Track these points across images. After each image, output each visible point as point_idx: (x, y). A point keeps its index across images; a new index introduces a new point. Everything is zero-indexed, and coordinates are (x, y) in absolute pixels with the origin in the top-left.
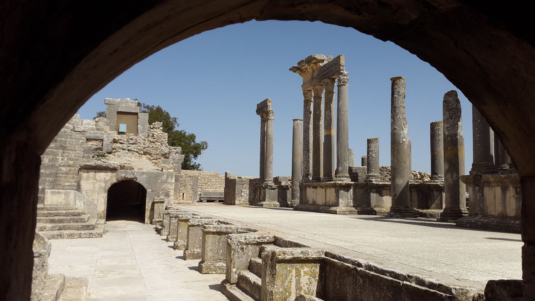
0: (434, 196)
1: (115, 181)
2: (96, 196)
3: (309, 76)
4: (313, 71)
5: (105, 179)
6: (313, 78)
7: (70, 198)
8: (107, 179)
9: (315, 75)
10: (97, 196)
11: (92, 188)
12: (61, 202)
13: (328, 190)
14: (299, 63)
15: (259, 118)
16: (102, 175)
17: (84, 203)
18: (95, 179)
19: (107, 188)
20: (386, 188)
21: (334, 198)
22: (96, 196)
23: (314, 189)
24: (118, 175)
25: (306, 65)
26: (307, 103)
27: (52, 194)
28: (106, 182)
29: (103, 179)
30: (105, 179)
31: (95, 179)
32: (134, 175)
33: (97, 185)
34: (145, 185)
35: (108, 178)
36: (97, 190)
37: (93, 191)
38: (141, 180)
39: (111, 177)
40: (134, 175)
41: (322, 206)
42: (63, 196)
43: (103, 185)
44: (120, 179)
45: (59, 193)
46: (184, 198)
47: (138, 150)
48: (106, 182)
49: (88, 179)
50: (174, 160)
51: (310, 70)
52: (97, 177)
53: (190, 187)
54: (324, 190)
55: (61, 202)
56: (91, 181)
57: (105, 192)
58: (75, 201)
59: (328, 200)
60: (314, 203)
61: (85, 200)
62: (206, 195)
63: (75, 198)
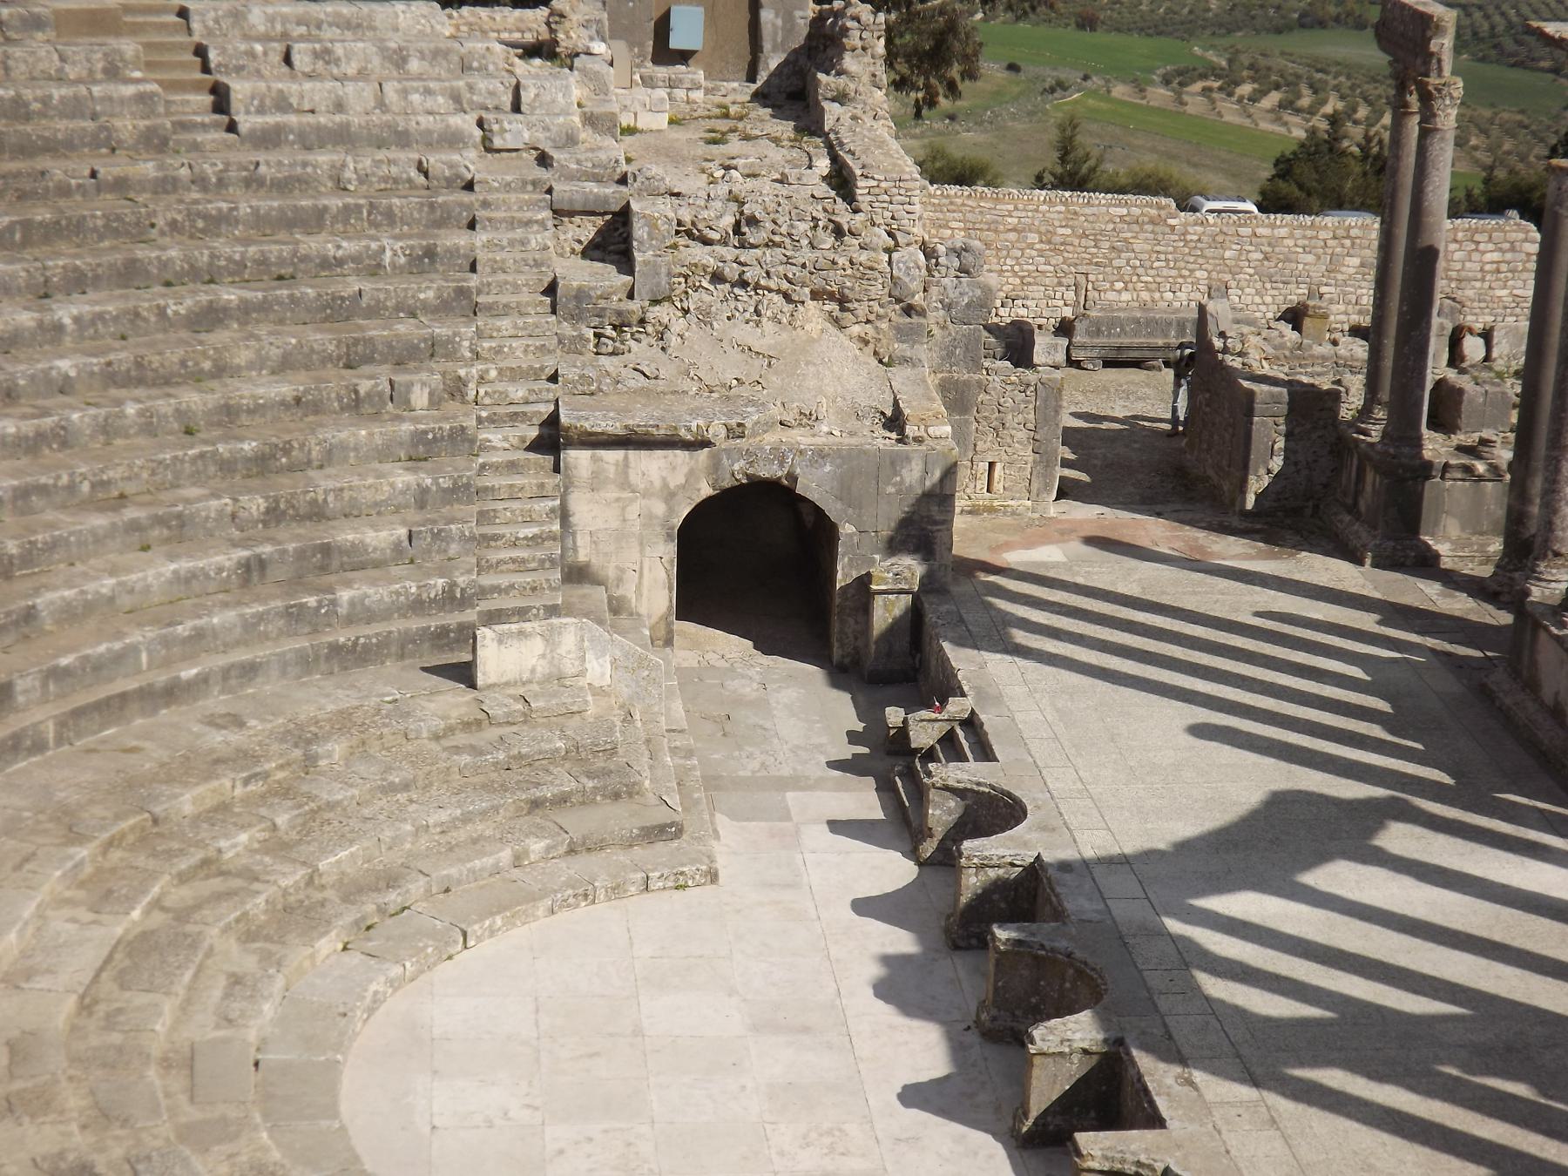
1: (706, 491)
2: (631, 556)
5: (665, 485)
7: (562, 650)
8: (674, 483)
10: (636, 556)
11: (615, 524)
12: (533, 671)
16: (651, 466)
17: (614, 662)
18: (625, 484)
19: (678, 521)
22: (631, 556)
24: (715, 466)
27: (500, 642)
28: (670, 496)
29: (658, 484)
30: (665, 485)
31: (625, 484)
32: (781, 465)
33: (633, 511)
34: (832, 509)
35: (677, 479)
36: (637, 529)
37: (620, 536)
38: (814, 486)
39: (691, 474)
40: (781, 465)
42: (538, 645)
43: (659, 508)
44: (727, 483)
45: (521, 633)
46: (998, 486)
47: (785, 285)
48: (670, 496)
49: (596, 482)
50: (948, 307)
52: (634, 478)
53: (1022, 435)
55: (533, 671)
56: (611, 493)
58: (583, 659)
61: (618, 654)
62: (1098, 332)
63: (581, 649)
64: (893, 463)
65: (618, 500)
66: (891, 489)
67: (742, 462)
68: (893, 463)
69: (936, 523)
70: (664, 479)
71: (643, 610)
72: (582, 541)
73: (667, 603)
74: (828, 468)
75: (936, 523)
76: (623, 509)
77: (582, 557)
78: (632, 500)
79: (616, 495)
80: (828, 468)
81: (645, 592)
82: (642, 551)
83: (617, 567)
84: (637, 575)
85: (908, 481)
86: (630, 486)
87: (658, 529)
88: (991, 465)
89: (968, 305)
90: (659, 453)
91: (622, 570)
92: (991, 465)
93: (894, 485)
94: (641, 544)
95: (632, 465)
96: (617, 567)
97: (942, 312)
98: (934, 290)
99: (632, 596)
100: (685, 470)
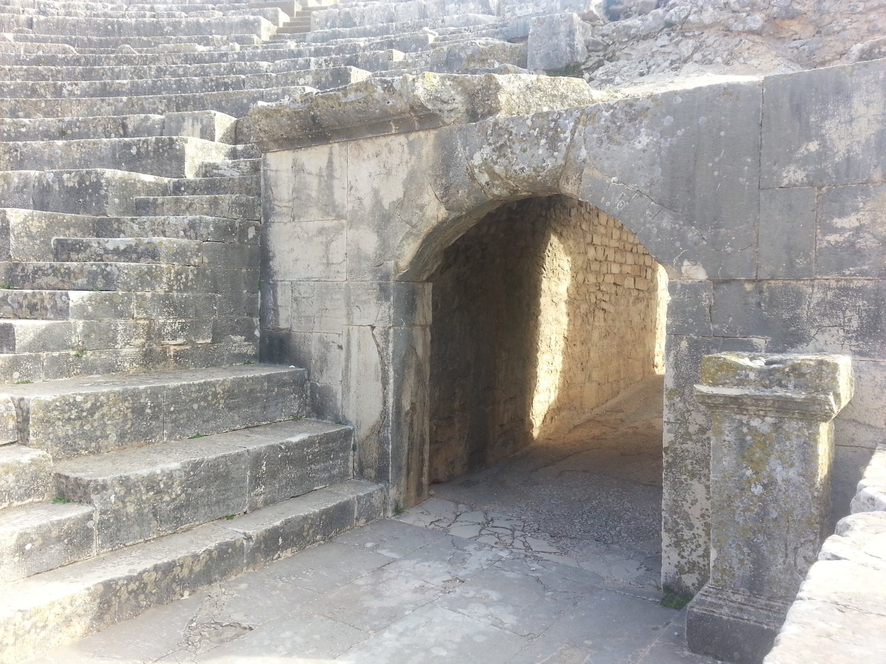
1: (434, 211)
5: (378, 203)
24: (446, 161)
28: (383, 220)
29: (368, 202)
30: (378, 203)
33: (339, 248)
43: (370, 242)
48: (383, 220)
52: (340, 195)
57: (383, 292)
64: (798, 110)
65: (321, 231)
66: (794, 175)
67: (487, 150)
70: (376, 192)
71: (351, 415)
72: (283, 297)
73: (379, 407)
74: (643, 140)
76: (327, 245)
77: (283, 325)
78: (338, 231)
79: (319, 224)
80: (643, 140)
81: (353, 383)
82: (349, 315)
83: (321, 340)
84: (343, 354)
85: (841, 147)
86: (335, 207)
87: (369, 277)
90: (369, 146)
91: (326, 345)
93: (805, 161)
94: (348, 305)
95: (337, 174)
96: (321, 340)
99: (338, 388)
100: (402, 174)
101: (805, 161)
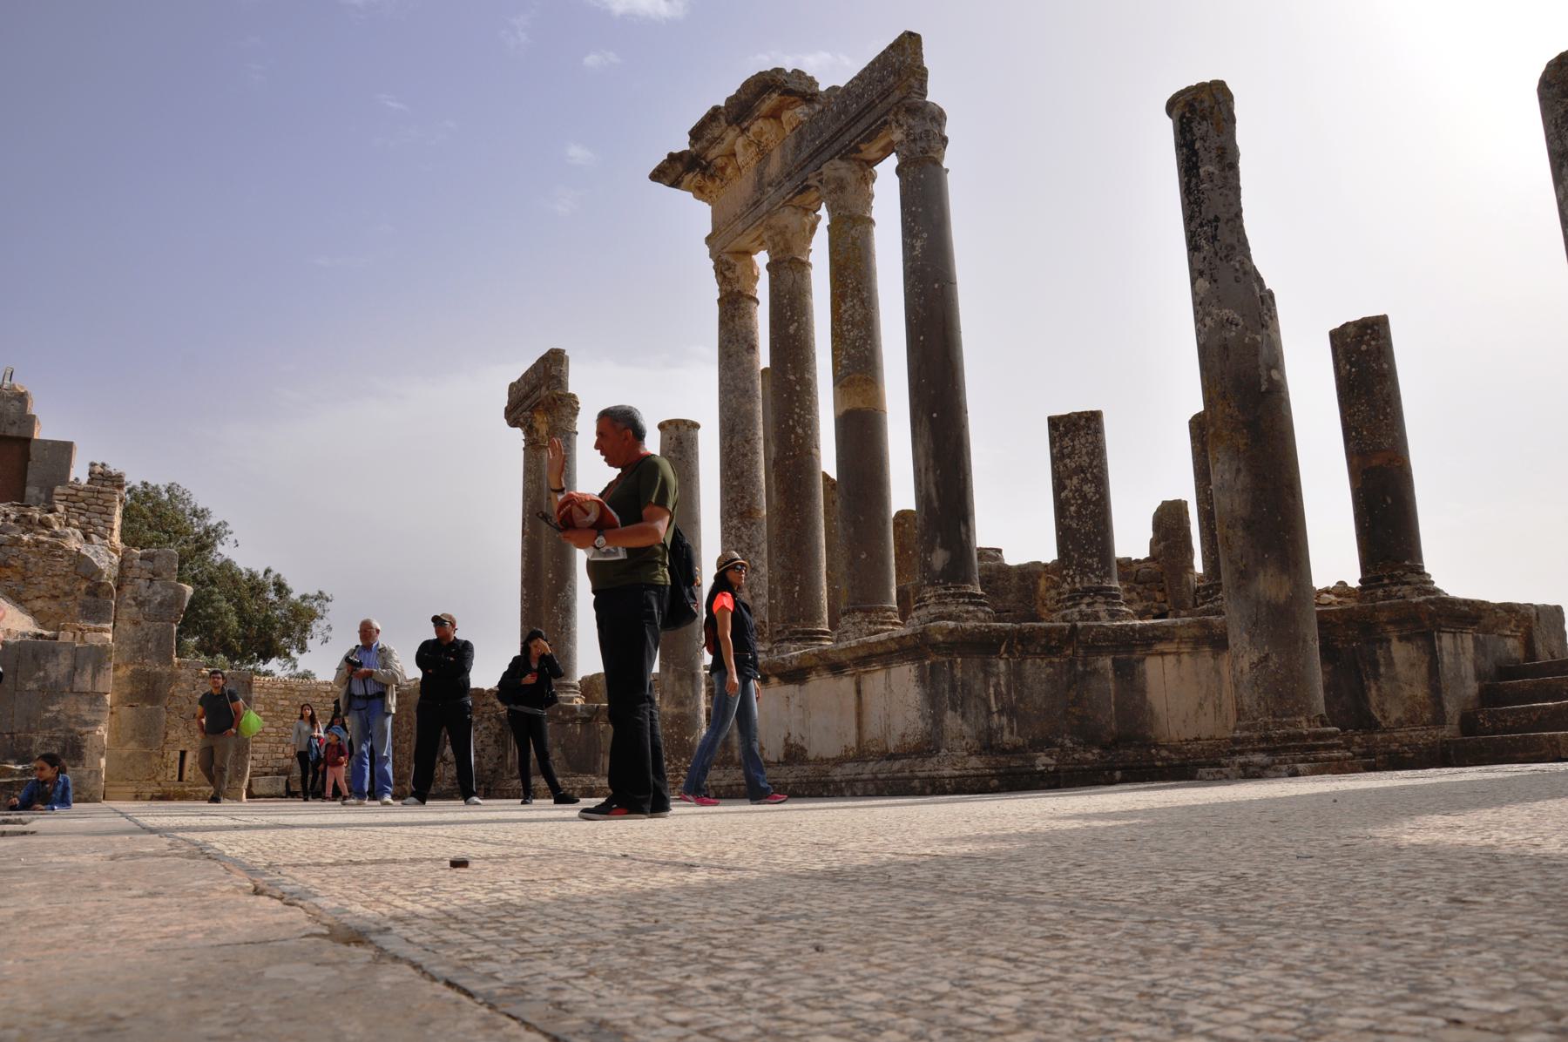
0: (1390, 663)
3: (741, 188)
4: (763, 155)
6: (760, 186)
9: (774, 168)
13: (876, 681)
14: (696, 134)
15: (518, 435)
20: (1159, 647)
21: (913, 715)
23: (791, 689)
25: (731, 134)
26: (734, 304)
41: (839, 761)
50: (141, 604)
51: (745, 156)
54: (846, 684)
59: (873, 729)
60: (794, 754)
64: (35, 657)
66: (32, 685)
68: (35, 657)
69: (86, 723)
75: (86, 723)
85: (53, 676)
88: (183, 754)
89: (161, 604)
92: (183, 754)
93: (37, 680)
97: (135, 609)
98: (128, 589)
101: (37, 680)
